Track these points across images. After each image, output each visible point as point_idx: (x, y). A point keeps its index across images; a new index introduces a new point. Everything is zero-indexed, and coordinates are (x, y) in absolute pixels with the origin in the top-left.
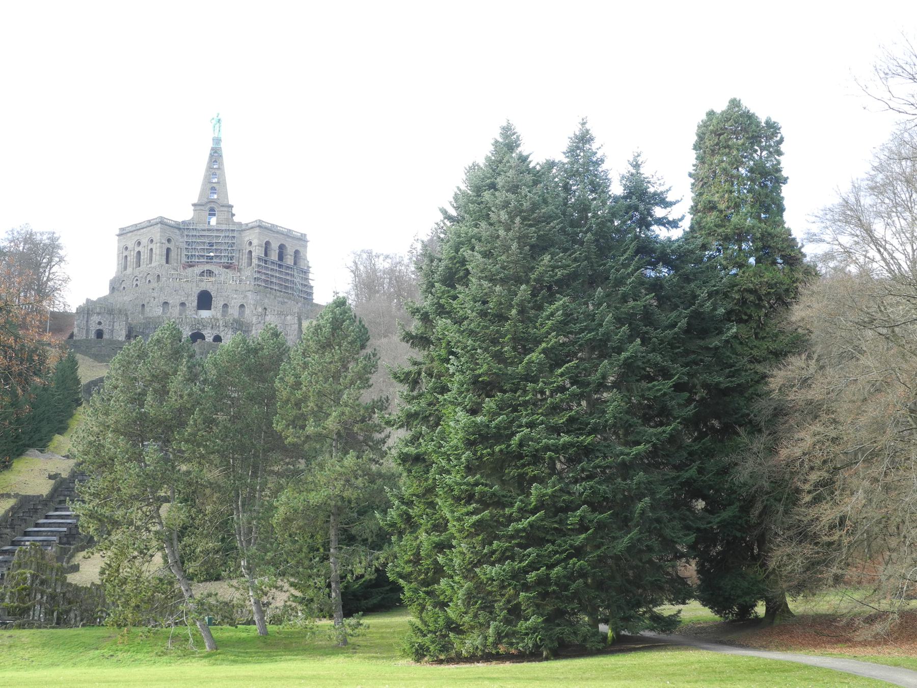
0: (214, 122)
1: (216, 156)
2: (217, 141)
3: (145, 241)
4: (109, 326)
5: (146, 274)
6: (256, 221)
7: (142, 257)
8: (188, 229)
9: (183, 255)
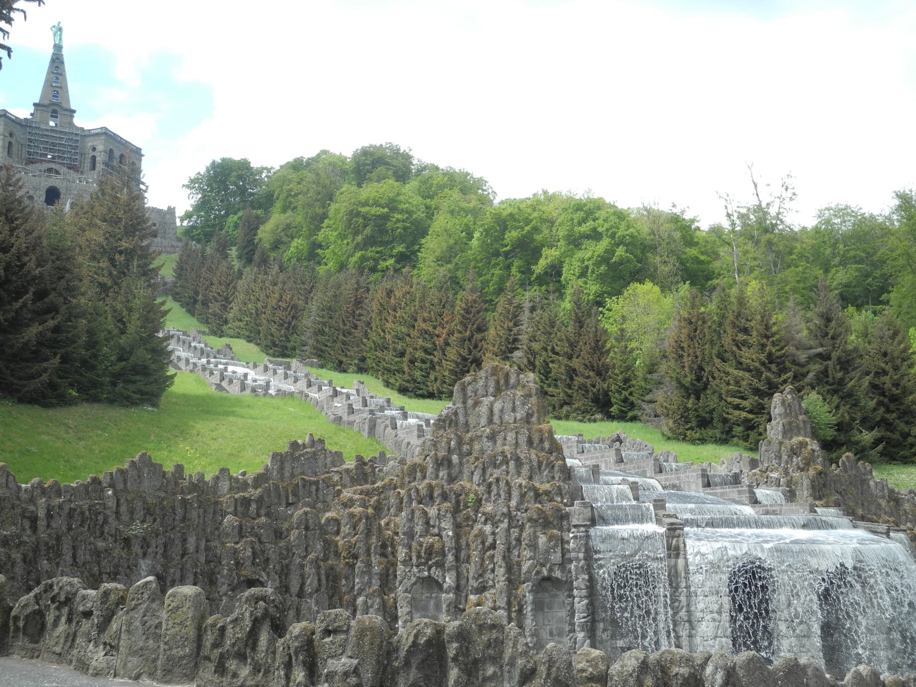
1: (57, 62)
2: (58, 48)
6: (102, 128)
8: (30, 127)
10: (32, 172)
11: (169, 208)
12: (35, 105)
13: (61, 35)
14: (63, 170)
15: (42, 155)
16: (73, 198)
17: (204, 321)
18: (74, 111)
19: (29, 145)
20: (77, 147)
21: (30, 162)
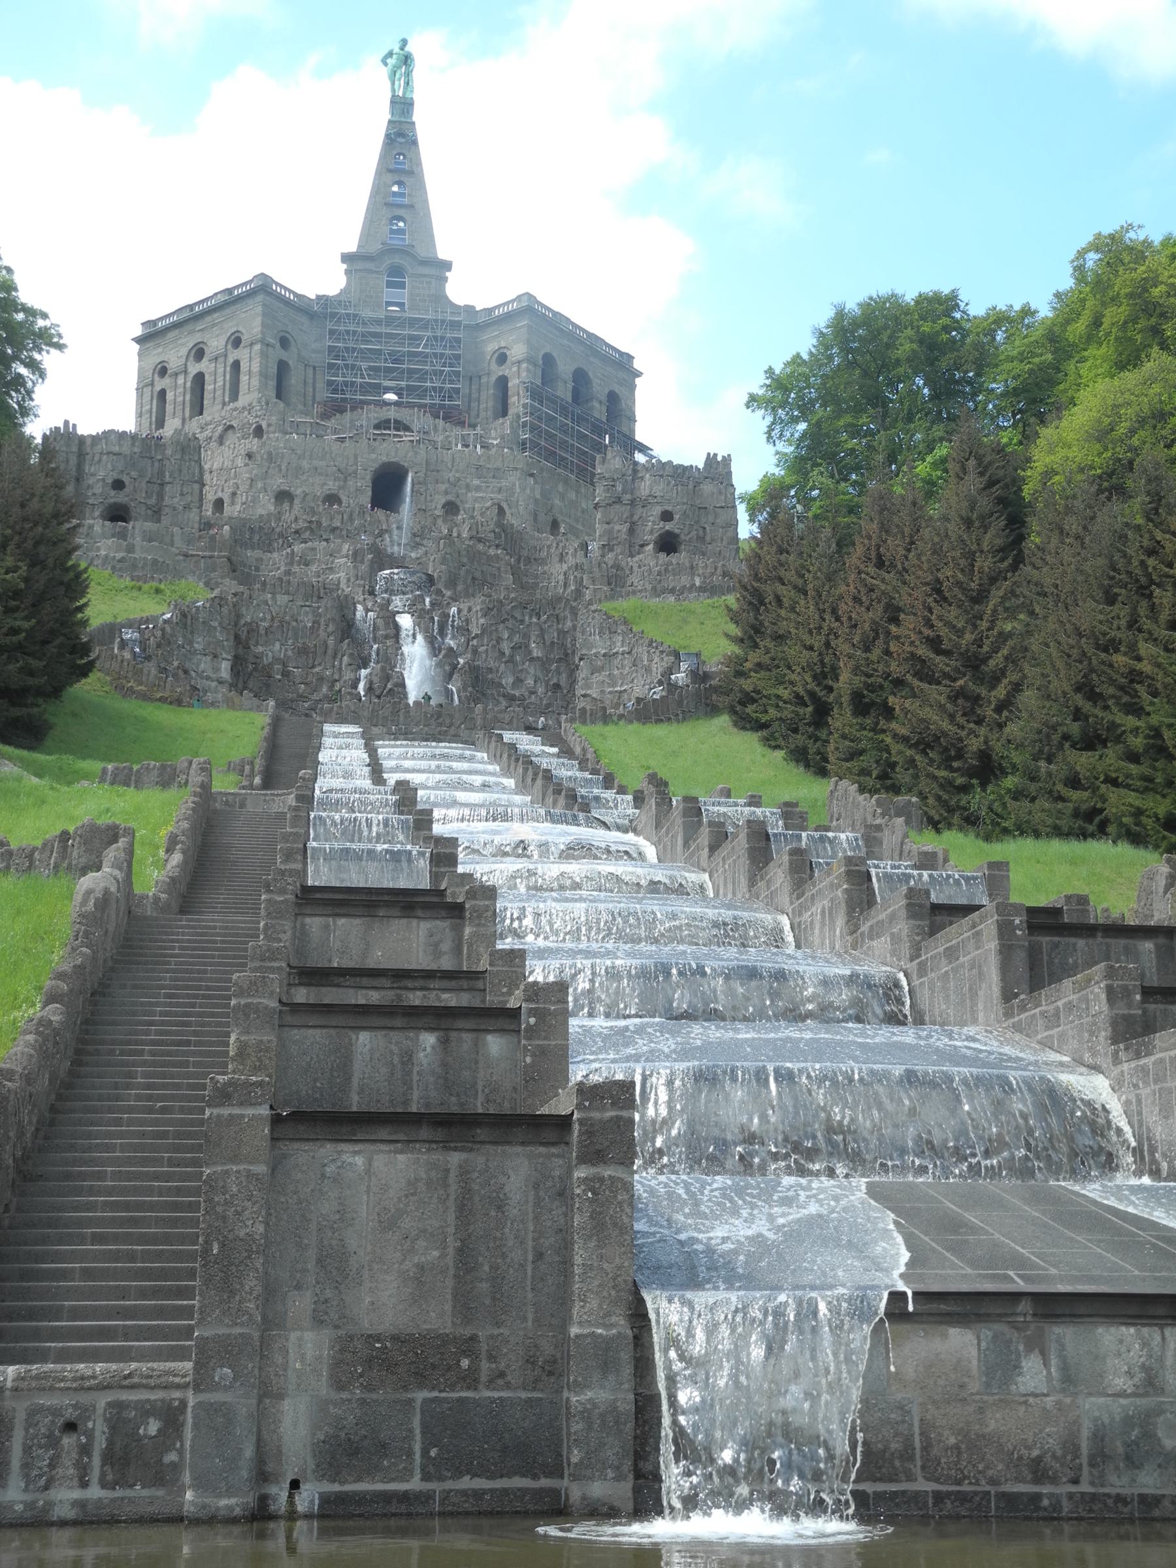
0: (391, 61)
2: (402, 106)
3: (216, 343)
4: (149, 495)
5: (220, 428)
6: (519, 298)
7: (209, 387)
8: (333, 315)
9: (320, 385)
10: (335, 432)
11: (711, 460)
12: (346, 258)
13: (408, 74)
14: (419, 420)
15: (365, 388)
16: (446, 493)
17: (870, 782)
18: (447, 266)
19: (331, 366)
20: (458, 357)
21: (335, 408)
